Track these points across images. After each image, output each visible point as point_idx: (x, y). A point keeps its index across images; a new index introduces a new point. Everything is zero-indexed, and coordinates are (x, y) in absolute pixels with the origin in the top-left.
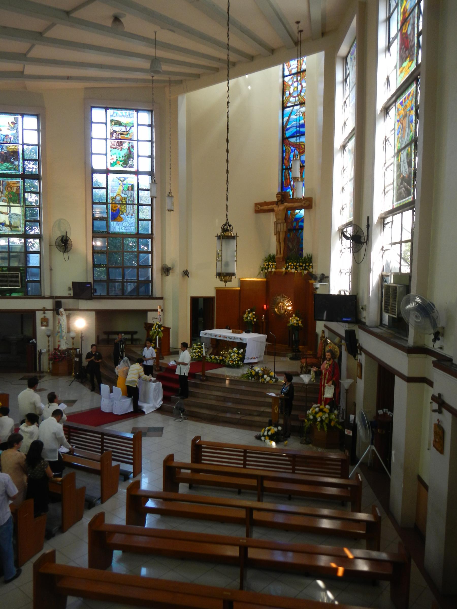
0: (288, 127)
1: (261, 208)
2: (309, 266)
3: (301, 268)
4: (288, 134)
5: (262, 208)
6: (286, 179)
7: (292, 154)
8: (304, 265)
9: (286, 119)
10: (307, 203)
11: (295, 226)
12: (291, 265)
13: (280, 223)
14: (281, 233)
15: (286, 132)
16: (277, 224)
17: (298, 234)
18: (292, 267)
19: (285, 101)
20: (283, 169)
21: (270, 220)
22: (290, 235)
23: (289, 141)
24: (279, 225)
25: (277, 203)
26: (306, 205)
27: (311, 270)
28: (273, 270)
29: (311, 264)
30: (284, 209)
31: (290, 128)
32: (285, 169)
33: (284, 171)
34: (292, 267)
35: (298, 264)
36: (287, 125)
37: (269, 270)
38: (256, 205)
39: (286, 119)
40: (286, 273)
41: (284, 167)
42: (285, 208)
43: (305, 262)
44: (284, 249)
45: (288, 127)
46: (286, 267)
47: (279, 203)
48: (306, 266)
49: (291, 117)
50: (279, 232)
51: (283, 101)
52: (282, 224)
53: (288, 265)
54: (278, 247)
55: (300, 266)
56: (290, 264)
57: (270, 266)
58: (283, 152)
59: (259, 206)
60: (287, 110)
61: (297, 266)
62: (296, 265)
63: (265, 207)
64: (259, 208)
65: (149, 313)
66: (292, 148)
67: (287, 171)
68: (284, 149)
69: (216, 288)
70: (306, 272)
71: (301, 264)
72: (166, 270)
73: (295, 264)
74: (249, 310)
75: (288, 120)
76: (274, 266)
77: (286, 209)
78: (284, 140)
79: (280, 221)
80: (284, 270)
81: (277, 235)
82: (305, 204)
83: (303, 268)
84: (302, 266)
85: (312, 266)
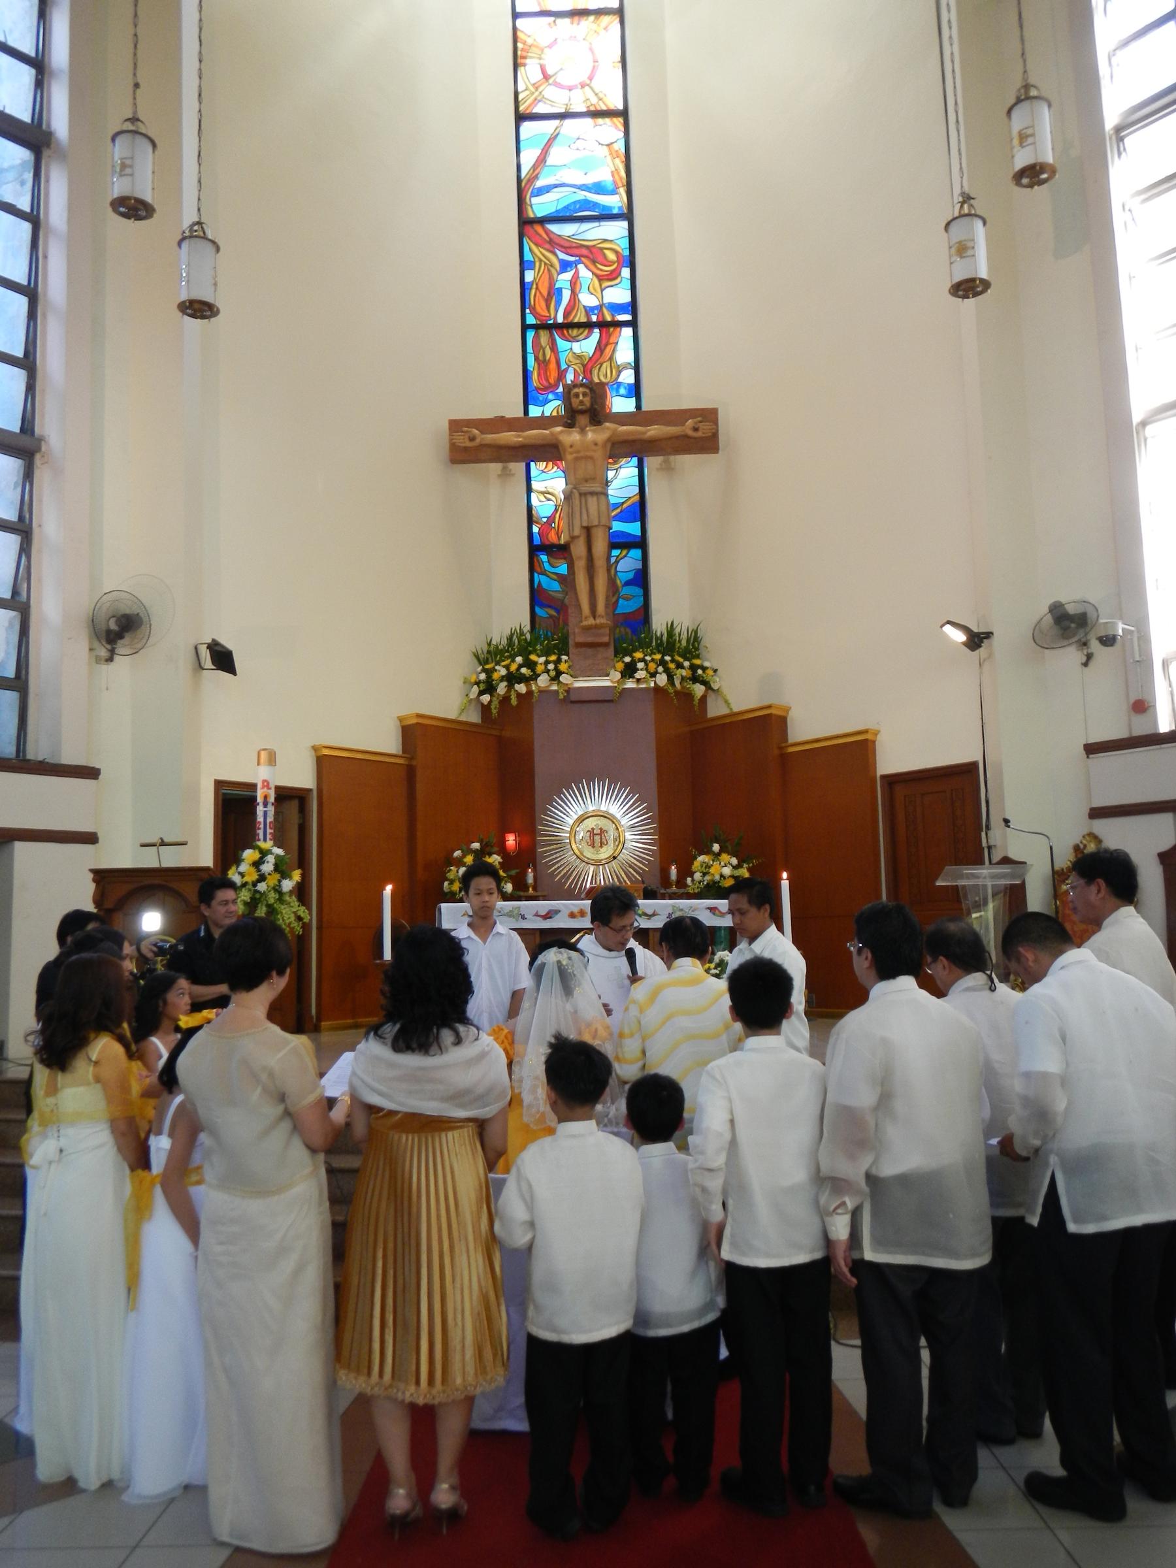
0: (539, 183)
1: (476, 445)
4: (540, 206)
5: (490, 438)
6: (542, 364)
7: (567, 276)
9: (528, 158)
10: (705, 429)
15: (534, 200)
18: (652, 666)
19: (521, 97)
20: (525, 328)
23: (547, 232)
26: (699, 434)
31: (548, 189)
33: (530, 334)
34: (652, 666)
36: (536, 177)
38: (456, 426)
39: (528, 158)
41: (531, 320)
42: (609, 440)
45: (539, 183)
46: (620, 666)
47: (583, 420)
49: (553, 151)
51: (516, 94)
56: (638, 655)
58: (523, 265)
60: (527, 127)
63: (510, 437)
64: (472, 439)
65: (19, 846)
66: (562, 256)
67: (544, 336)
68: (528, 256)
69: (315, 749)
72: (119, 630)
73: (658, 657)
74: (476, 845)
75: (541, 160)
77: (609, 446)
78: (526, 223)
82: (696, 429)
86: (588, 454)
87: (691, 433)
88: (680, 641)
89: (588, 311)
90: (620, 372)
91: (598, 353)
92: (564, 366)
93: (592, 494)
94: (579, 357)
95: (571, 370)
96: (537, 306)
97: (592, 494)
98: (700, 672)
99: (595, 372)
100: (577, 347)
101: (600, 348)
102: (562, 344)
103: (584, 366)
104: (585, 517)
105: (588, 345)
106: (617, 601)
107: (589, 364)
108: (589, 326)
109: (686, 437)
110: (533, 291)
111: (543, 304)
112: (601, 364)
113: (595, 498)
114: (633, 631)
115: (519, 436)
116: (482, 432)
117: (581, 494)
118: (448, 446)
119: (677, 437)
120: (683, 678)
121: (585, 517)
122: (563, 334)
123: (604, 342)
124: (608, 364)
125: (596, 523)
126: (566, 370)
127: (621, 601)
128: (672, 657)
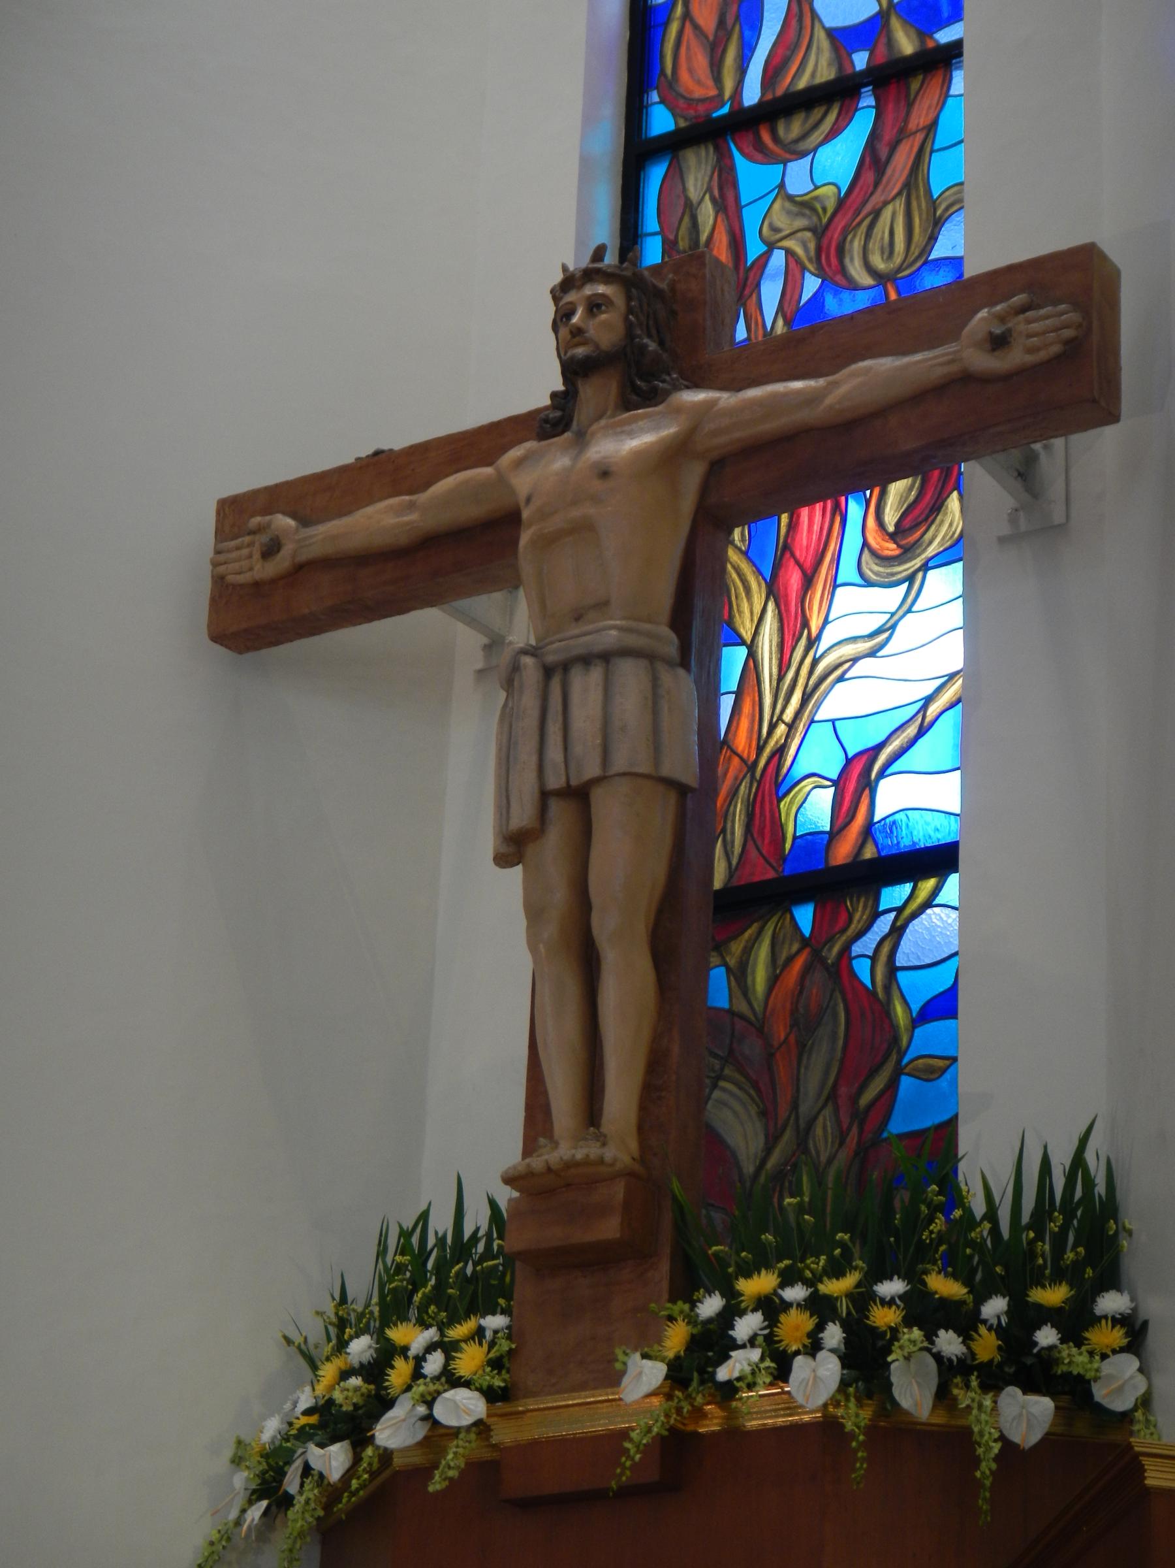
1: (304, 575)
2: (1076, 1322)
3: (949, 1343)
8: (995, 1307)
10: (1041, 332)
11: (813, 843)
12: (771, 1307)
13: (606, 657)
14: (612, 811)
16: (556, 671)
17: (866, 944)
18: (795, 1324)
20: (638, 152)
21: (422, 745)
22: (740, 975)
24: (586, 687)
25: (556, 421)
27: (1118, 1382)
28: (462, 1407)
29: (1111, 1303)
30: (670, 457)
32: (673, 145)
33: (656, 175)
34: (795, 1324)
35: (892, 1287)
37: (394, 1432)
38: (236, 514)
40: (676, 1446)
43: (1007, 1264)
44: (656, 1063)
46: (676, 1338)
48: (1025, 1318)
50: (579, 795)
52: (631, 678)
53: (711, 1306)
54: (562, 1035)
55: (925, 1312)
57: (399, 1373)
59: (284, 522)
61: (884, 1317)
62: (863, 1298)
70: (1026, 1415)
71: (943, 1286)
76: (470, 1361)
77: (693, 476)
79: (608, 633)
80: (645, 1376)
81: (553, 845)
82: (998, 342)
83: (987, 1346)
84: (965, 1321)
85: (1136, 1332)
86: (576, 513)
87: (983, 362)
88: (991, 1214)
89: (844, 39)
90: (936, 224)
91: (869, 176)
92: (754, 249)
93: (586, 660)
94: (804, 205)
95: (778, 259)
96: (684, 76)
97: (586, 660)
98: (1046, 1336)
99: (856, 245)
100: (797, 177)
101: (873, 160)
102: (753, 177)
103: (820, 232)
104: (555, 753)
105: (837, 159)
106: (893, 1085)
107: (830, 231)
108: (839, 94)
109: (966, 379)
110: (674, 28)
111: (701, 61)
112: (877, 214)
113: (596, 674)
114: (890, 1198)
115: (412, 506)
116: (305, 522)
117: (548, 672)
118: (205, 588)
119: (939, 390)
120: (949, 1370)
121: (555, 753)
122: (759, 147)
123: (888, 135)
124: (899, 205)
125: (592, 770)
126: (763, 261)
127: (906, 1082)
128: (914, 1277)
